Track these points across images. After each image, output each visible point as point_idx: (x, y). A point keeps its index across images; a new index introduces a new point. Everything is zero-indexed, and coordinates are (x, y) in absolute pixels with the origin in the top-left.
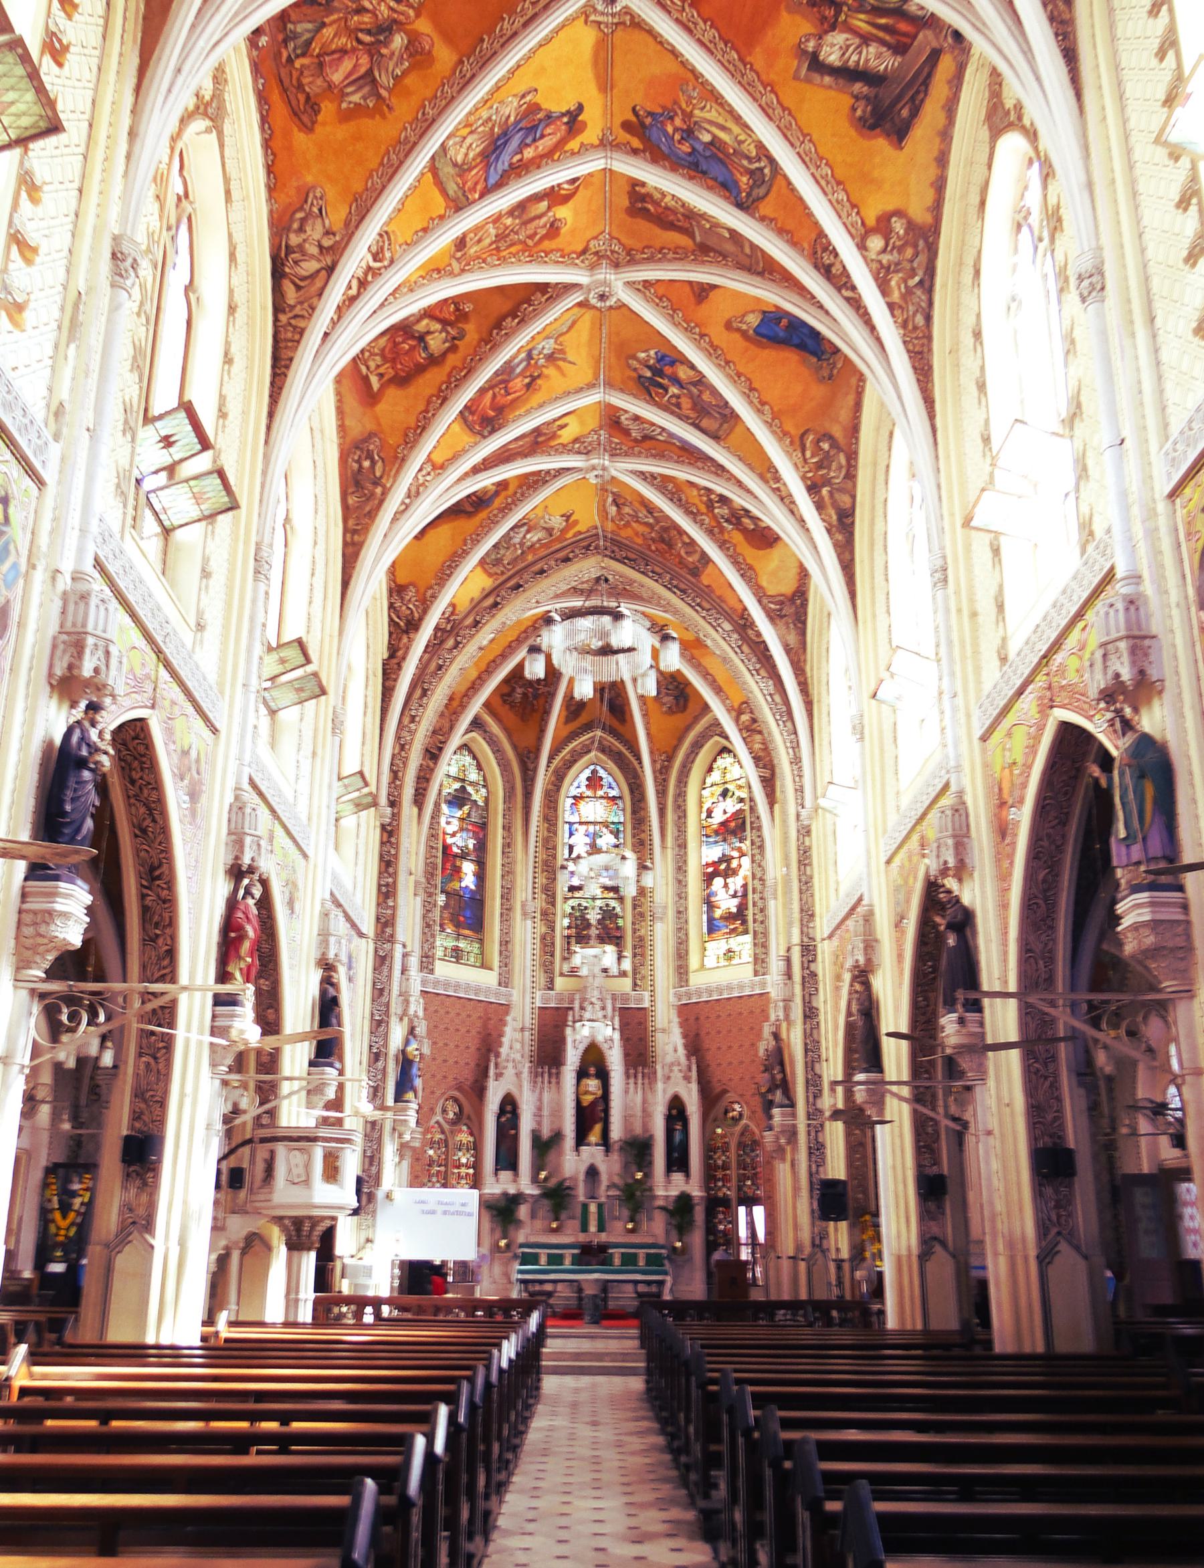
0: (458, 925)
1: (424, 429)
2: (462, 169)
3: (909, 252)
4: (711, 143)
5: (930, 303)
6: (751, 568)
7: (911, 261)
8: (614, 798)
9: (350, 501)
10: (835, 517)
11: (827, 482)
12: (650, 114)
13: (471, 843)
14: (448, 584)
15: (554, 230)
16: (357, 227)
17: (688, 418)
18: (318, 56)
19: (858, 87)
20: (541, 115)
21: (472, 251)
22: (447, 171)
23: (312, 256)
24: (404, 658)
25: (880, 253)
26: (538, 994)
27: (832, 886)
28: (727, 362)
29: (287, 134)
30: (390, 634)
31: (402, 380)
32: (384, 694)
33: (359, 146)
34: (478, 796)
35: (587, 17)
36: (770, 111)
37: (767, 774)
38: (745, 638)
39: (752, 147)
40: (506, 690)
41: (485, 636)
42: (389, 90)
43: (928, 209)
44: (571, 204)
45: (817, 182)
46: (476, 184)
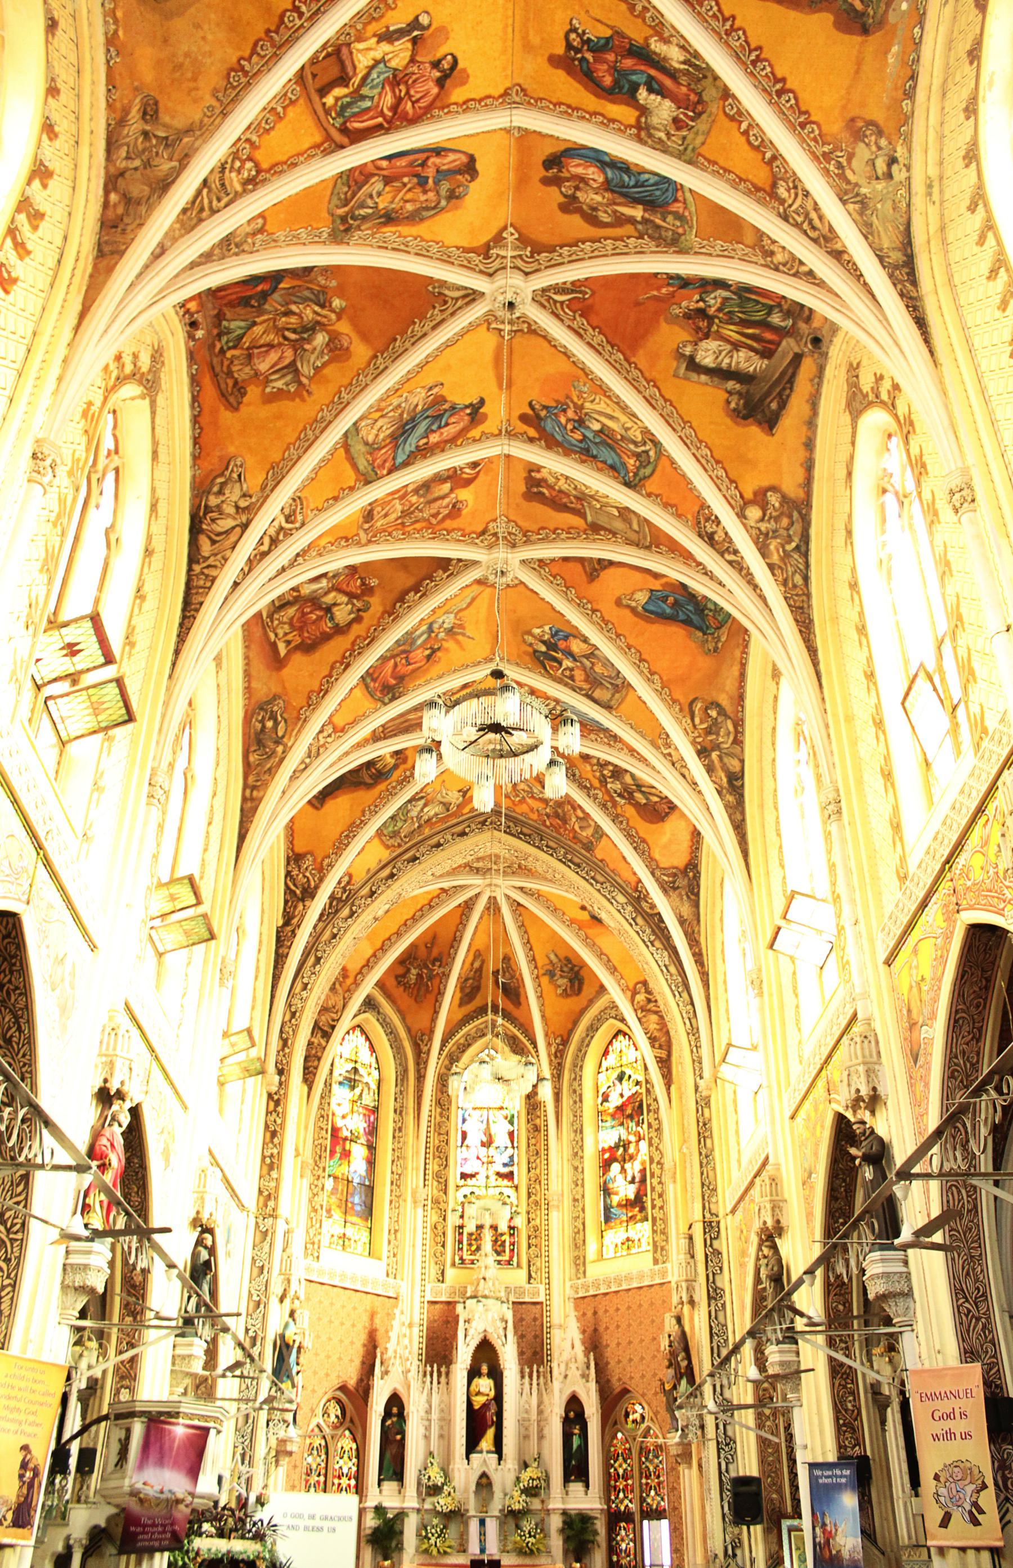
1: (327, 692)
2: (373, 448)
3: (785, 522)
4: (601, 431)
5: (807, 565)
6: (644, 841)
7: (788, 529)
9: (251, 759)
10: (725, 780)
11: (717, 747)
12: (545, 407)
14: (345, 853)
15: (455, 510)
16: (272, 491)
17: (581, 689)
18: (248, 349)
19: (731, 384)
20: (446, 406)
21: (379, 524)
22: (358, 449)
23: (229, 515)
25: (758, 522)
27: (734, 1156)
28: (618, 636)
29: (215, 412)
30: (286, 902)
31: (308, 648)
32: (276, 962)
33: (279, 424)
34: (371, 1078)
35: (489, 324)
36: (653, 402)
37: (663, 1054)
38: (639, 911)
39: (638, 434)
40: (401, 970)
41: (379, 906)
42: (310, 379)
43: (800, 485)
44: (472, 486)
45: (698, 460)
46: (385, 461)
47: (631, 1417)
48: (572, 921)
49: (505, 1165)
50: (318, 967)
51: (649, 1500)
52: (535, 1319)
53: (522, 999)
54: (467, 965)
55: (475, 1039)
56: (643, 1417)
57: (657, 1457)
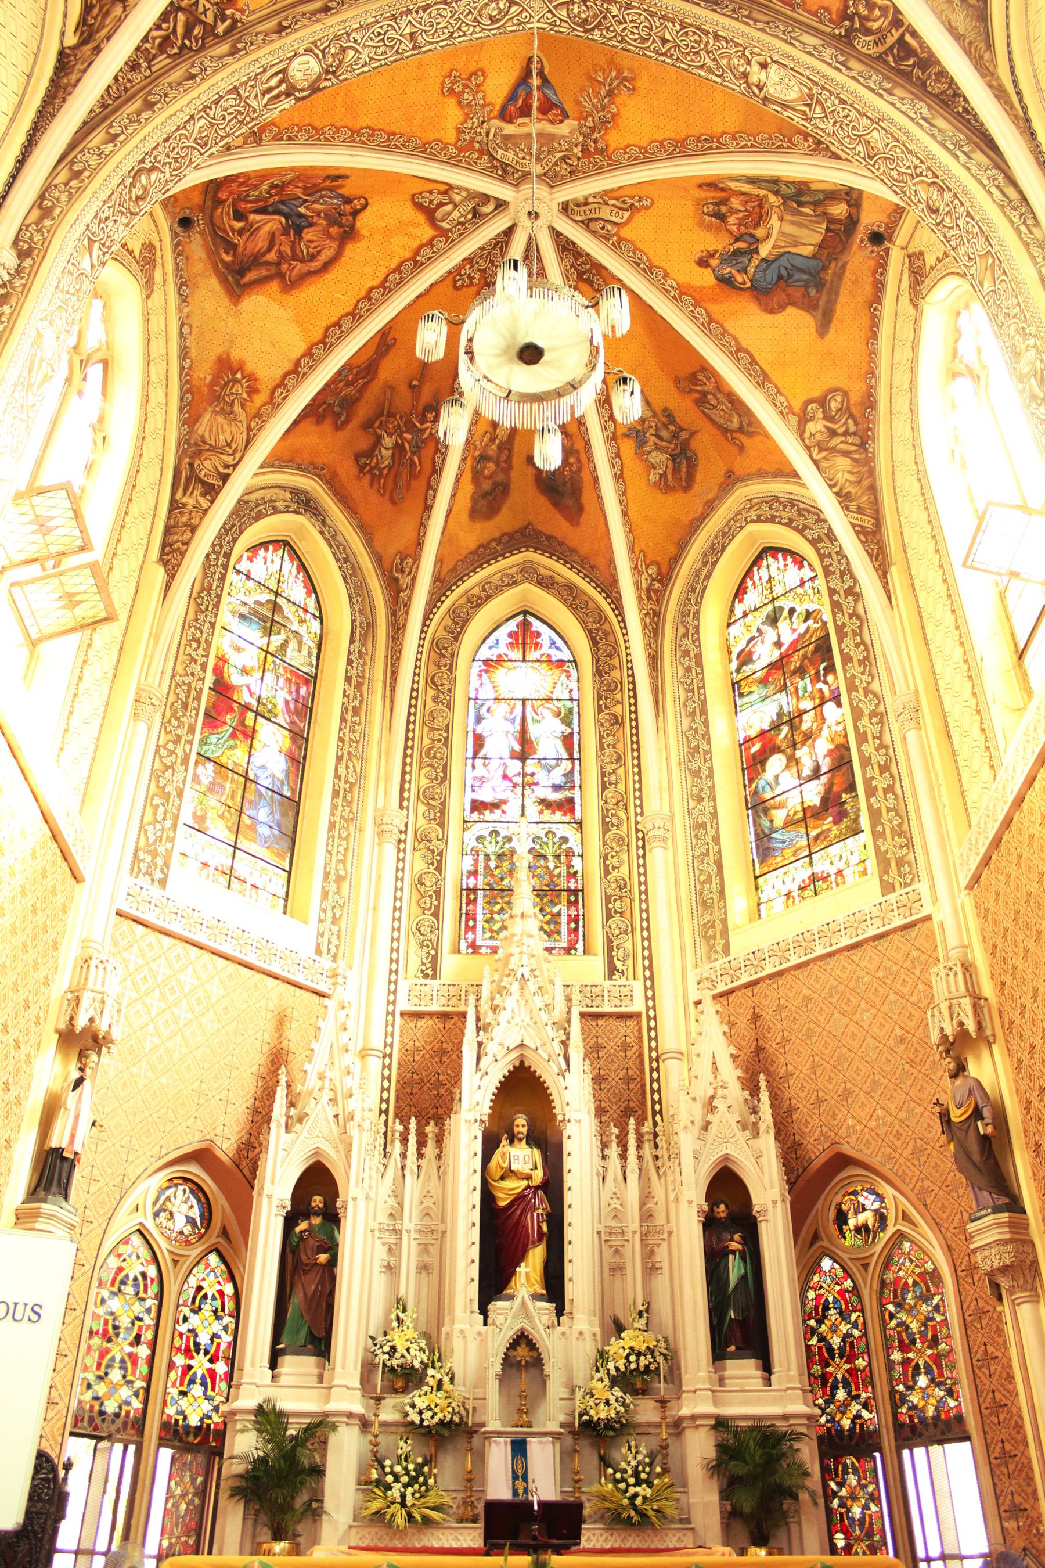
8: (561, 663)
24: (109, 38)
26: (403, 987)
37: (868, 523)
40: (364, 443)
47: (852, 1223)
49: (557, 788)
50: (145, 115)
51: (915, 1398)
52: (625, 1047)
53: (587, 497)
55: (499, 589)
56: (881, 1218)
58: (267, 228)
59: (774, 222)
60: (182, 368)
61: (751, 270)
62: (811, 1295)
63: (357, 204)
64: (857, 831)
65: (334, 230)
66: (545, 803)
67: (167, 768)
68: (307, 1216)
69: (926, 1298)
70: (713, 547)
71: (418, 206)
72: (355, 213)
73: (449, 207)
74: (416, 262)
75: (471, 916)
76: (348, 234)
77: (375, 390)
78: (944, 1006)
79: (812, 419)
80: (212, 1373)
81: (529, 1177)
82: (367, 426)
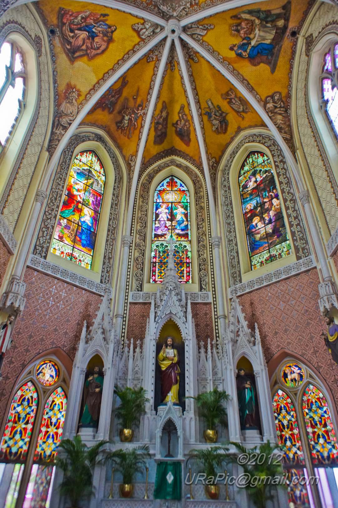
0: (74, 241)
8: (184, 191)
13: (91, 199)
26: (130, 294)
37: (288, 137)
40: (119, 119)
47: (289, 377)
48: (224, 59)
49: (182, 230)
51: (319, 447)
52: (206, 314)
53: (192, 136)
54: (158, 112)
55: (164, 168)
56: (301, 376)
57: (320, 408)
58: (82, 36)
59: (257, 31)
60: (55, 87)
61: (248, 51)
62: (275, 404)
63: (113, 28)
64: (286, 240)
65: (105, 38)
66: (178, 235)
67: (48, 219)
68: (93, 374)
69: (320, 408)
70: (233, 152)
71: (134, 30)
72: (112, 32)
73: (144, 30)
74: (134, 51)
75: (154, 271)
76: (110, 40)
77: (122, 99)
78: (325, 298)
79: (269, 103)
80: (57, 433)
81: (173, 360)
82: (120, 112)
